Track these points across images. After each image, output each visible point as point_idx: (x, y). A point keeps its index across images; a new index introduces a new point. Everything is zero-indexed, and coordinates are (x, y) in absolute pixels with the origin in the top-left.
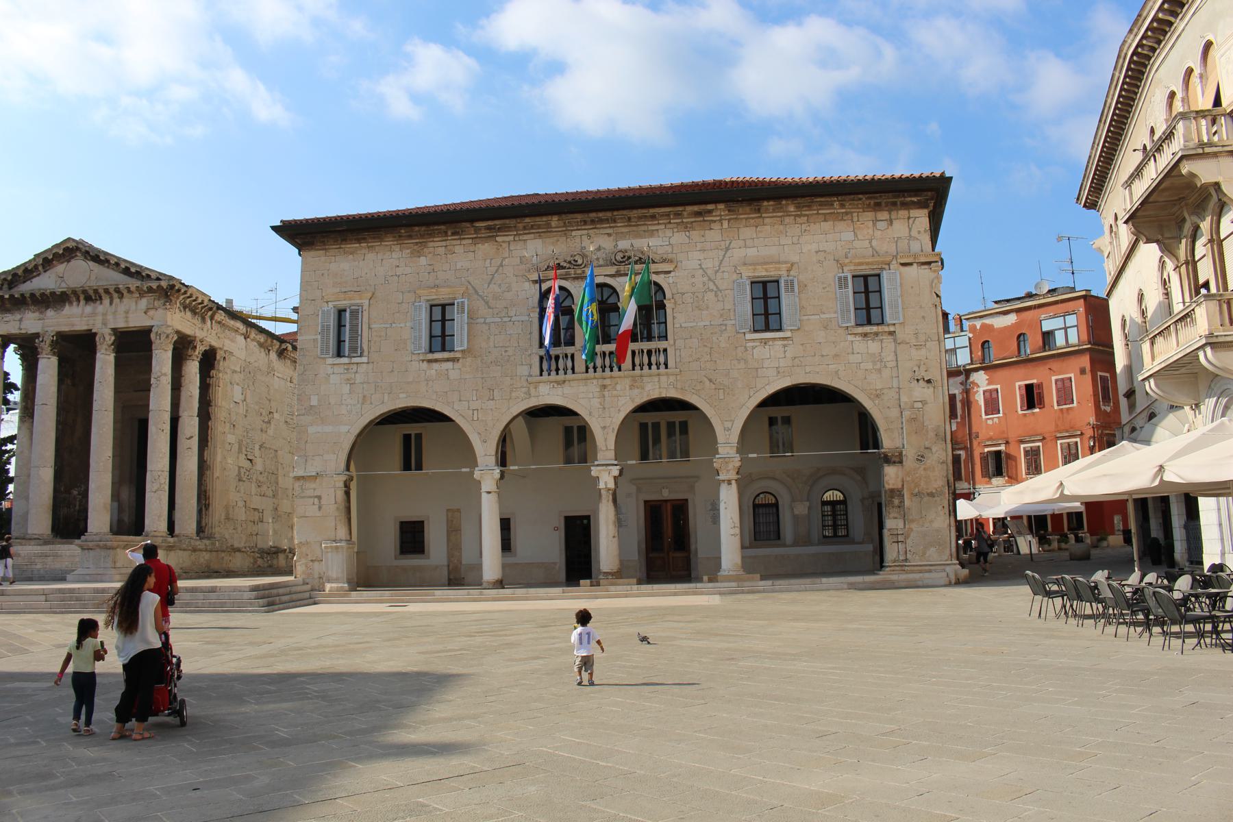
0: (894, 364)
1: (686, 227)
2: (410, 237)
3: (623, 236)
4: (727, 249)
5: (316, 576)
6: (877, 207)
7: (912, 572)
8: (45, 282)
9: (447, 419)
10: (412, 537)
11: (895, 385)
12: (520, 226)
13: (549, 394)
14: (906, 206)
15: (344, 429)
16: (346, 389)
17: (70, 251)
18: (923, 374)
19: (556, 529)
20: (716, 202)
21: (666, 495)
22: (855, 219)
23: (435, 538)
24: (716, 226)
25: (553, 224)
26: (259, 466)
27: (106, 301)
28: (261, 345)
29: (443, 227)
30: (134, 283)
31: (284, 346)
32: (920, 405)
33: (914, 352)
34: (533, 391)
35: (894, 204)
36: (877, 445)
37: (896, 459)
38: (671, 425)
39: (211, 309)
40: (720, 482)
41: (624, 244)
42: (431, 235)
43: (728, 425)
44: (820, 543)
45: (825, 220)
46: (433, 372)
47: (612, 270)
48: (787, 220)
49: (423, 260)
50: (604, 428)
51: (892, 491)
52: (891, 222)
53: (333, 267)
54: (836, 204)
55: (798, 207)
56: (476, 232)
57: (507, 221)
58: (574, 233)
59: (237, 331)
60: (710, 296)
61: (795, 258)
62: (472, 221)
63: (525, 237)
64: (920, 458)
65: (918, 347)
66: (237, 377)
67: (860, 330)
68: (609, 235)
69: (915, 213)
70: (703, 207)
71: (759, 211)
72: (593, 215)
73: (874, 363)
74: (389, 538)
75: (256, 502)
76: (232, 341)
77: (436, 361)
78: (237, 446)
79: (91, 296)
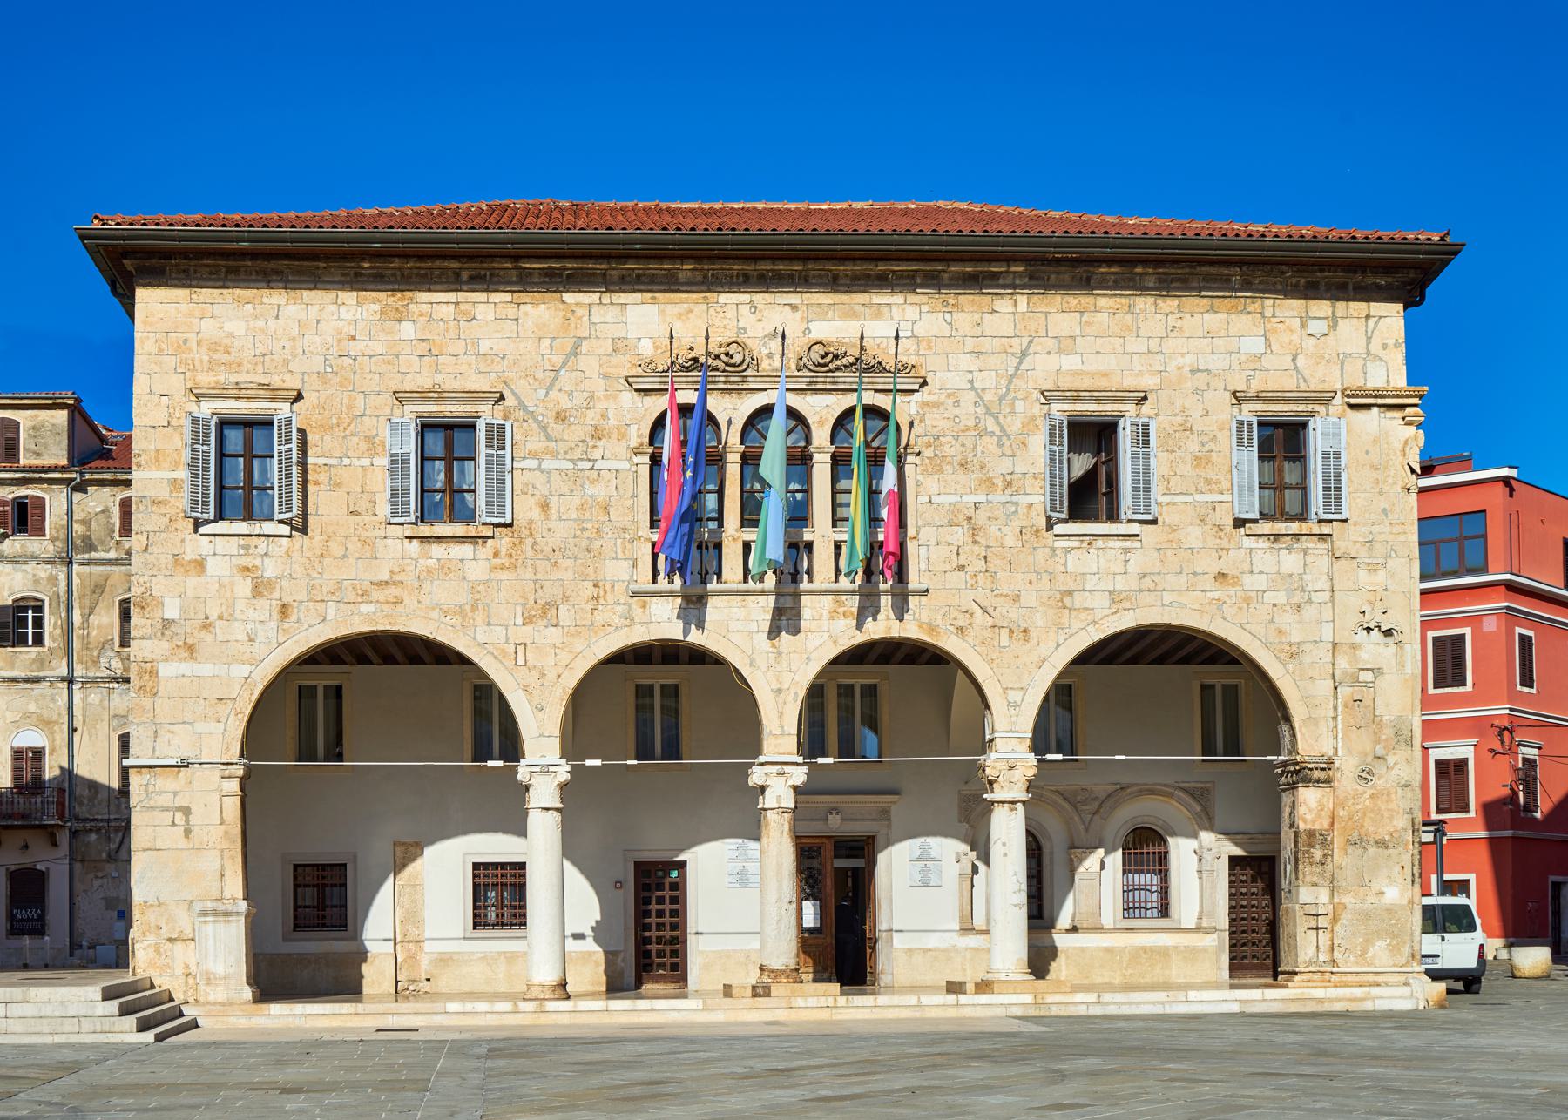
0: (1328, 594)
3: (822, 312)
4: (1024, 354)
5: (179, 971)
7: (1347, 985)
9: (463, 660)
11: (1328, 636)
16: (244, 587)
18: (1379, 617)
20: (1010, 259)
22: (1268, 312)
25: (681, 275)
29: (454, 264)
34: (638, 612)
43: (1015, 696)
49: (407, 330)
50: (779, 691)
52: (1333, 322)
53: (208, 327)
60: (989, 443)
61: (1148, 382)
62: (516, 258)
64: (1365, 777)
65: (1373, 567)
67: (1266, 528)
68: (794, 308)
69: (1378, 308)
72: (764, 266)
77: (439, 539)
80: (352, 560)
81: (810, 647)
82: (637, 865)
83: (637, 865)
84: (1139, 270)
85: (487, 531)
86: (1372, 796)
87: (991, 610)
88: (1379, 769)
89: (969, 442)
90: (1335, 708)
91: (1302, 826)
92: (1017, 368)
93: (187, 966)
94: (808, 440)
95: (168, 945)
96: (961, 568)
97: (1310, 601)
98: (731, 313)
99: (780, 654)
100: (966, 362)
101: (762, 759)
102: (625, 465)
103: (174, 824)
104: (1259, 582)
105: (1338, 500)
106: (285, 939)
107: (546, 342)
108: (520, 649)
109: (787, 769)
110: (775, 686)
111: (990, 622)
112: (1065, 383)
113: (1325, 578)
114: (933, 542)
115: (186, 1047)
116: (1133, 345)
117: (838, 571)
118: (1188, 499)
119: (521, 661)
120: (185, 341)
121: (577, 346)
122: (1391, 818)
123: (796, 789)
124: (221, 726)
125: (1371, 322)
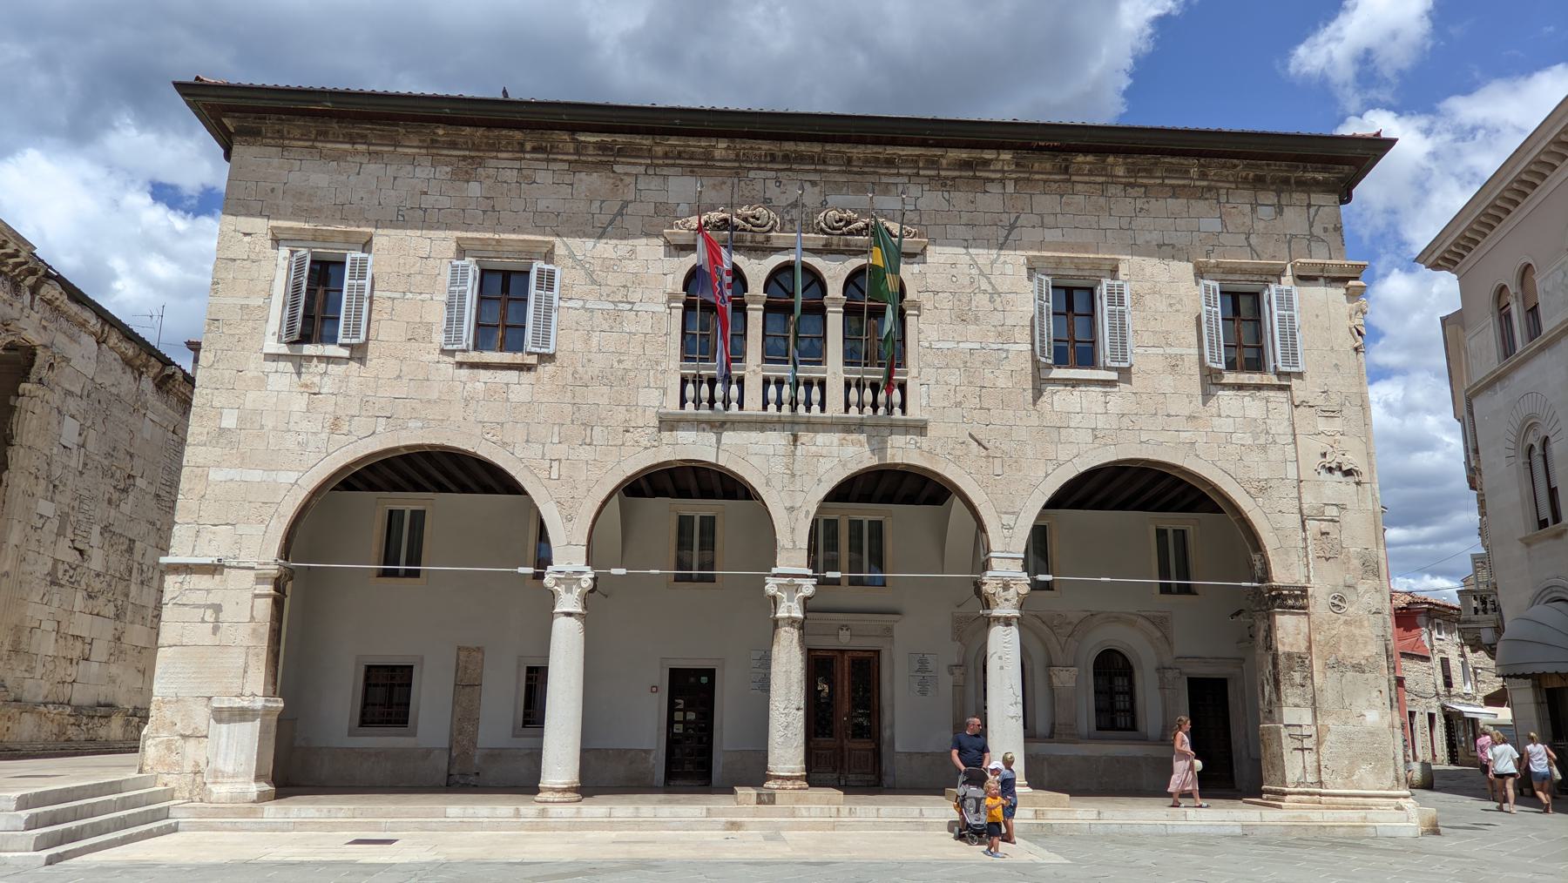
1: (944, 184)
2: (453, 145)
4: (1012, 227)
5: (188, 768)
6: (1259, 183)
10: (386, 696)
11: (1292, 472)
12: (659, 150)
13: (694, 446)
14: (1306, 186)
15: (288, 477)
16: (300, 402)
19: (655, 689)
20: (999, 147)
21: (845, 640)
22: (1223, 199)
23: (431, 701)
24: (994, 188)
25: (717, 154)
26: (96, 562)
28: (127, 362)
29: (518, 135)
31: (168, 371)
32: (1333, 512)
33: (1322, 425)
35: (1286, 181)
36: (1266, 575)
37: (1295, 600)
38: (856, 526)
39: (33, 272)
40: (988, 622)
42: (494, 147)
43: (1006, 519)
44: (1091, 738)
45: (1174, 196)
46: (480, 386)
47: (816, 239)
48: (1112, 190)
49: (474, 189)
50: (791, 509)
51: (1289, 656)
52: (1280, 210)
53: (295, 178)
54: (1194, 172)
55: (1132, 171)
56: (577, 152)
57: (637, 139)
58: (752, 174)
59: (83, 325)
60: (982, 301)
62: (573, 129)
63: (666, 171)
64: (1338, 603)
65: (1330, 414)
66: (72, 405)
70: (976, 154)
71: (1066, 170)
72: (789, 146)
73: (1255, 436)
74: (341, 698)
75: (82, 625)
76: (72, 338)
77: (486, 366)
78: (54, 525)
80: (405, 381)
81: (821, 471)
82: (672, 670)
83: (672, 670)
84: (1111, 159)
85: (533, 360)
86: (1346, 622)
87: (985, 443)
88: (1350, 596)
89: (965, 299)
90: (1305, 539)
91: (1281, 649)
92: (1007, 238)
93: (197, 765)
94: (824, 292)
95: (180, 742)
96: (958, 404)
97: (1275, 442)
98: (759, 186)
99: (793, 475)
101: (774, 571)
102: (662, 308)
103: (203, 621)
104: (1225, 425)
105: (1295, 354)
106: (350, 734)
107: (597, 204)
108: (555, 464)
109: (798, 581)
110: (788, 505)
111: (984, 453)
113: (1286, 423)
114: (932, 382)
115: (104, 869)
117: (847, 407)
118: (1161, 351)
119: (554, 475)
120: (273, 190)
121: (622, 208)
122: (1366, 643)
123: (806, 599)
124: (263, 527)
125: (1312, 210)
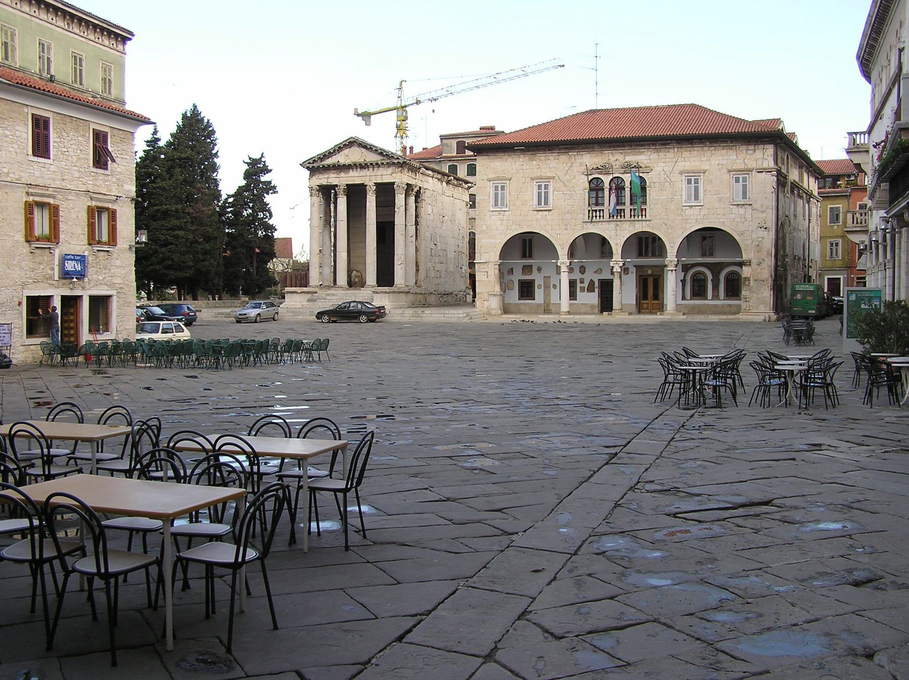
1: (657, 151)
8: (340, 159)
14: (763, 143)
17: (352, 143)
27: (371, 169)
30: (386, 161)
33: (760, 215)
37: (748, 263)
41: (628, 158)
49: (534, 162)
53: (492, 164)
61: (707, 167)
64: (759, 264)
65: (763, 212)
69: (766, 146)
79: (363, 166)
91: (743, 276)
100: (662, 164)
104: (733, 216)
112: (687, 168)
116: (704, 159)
